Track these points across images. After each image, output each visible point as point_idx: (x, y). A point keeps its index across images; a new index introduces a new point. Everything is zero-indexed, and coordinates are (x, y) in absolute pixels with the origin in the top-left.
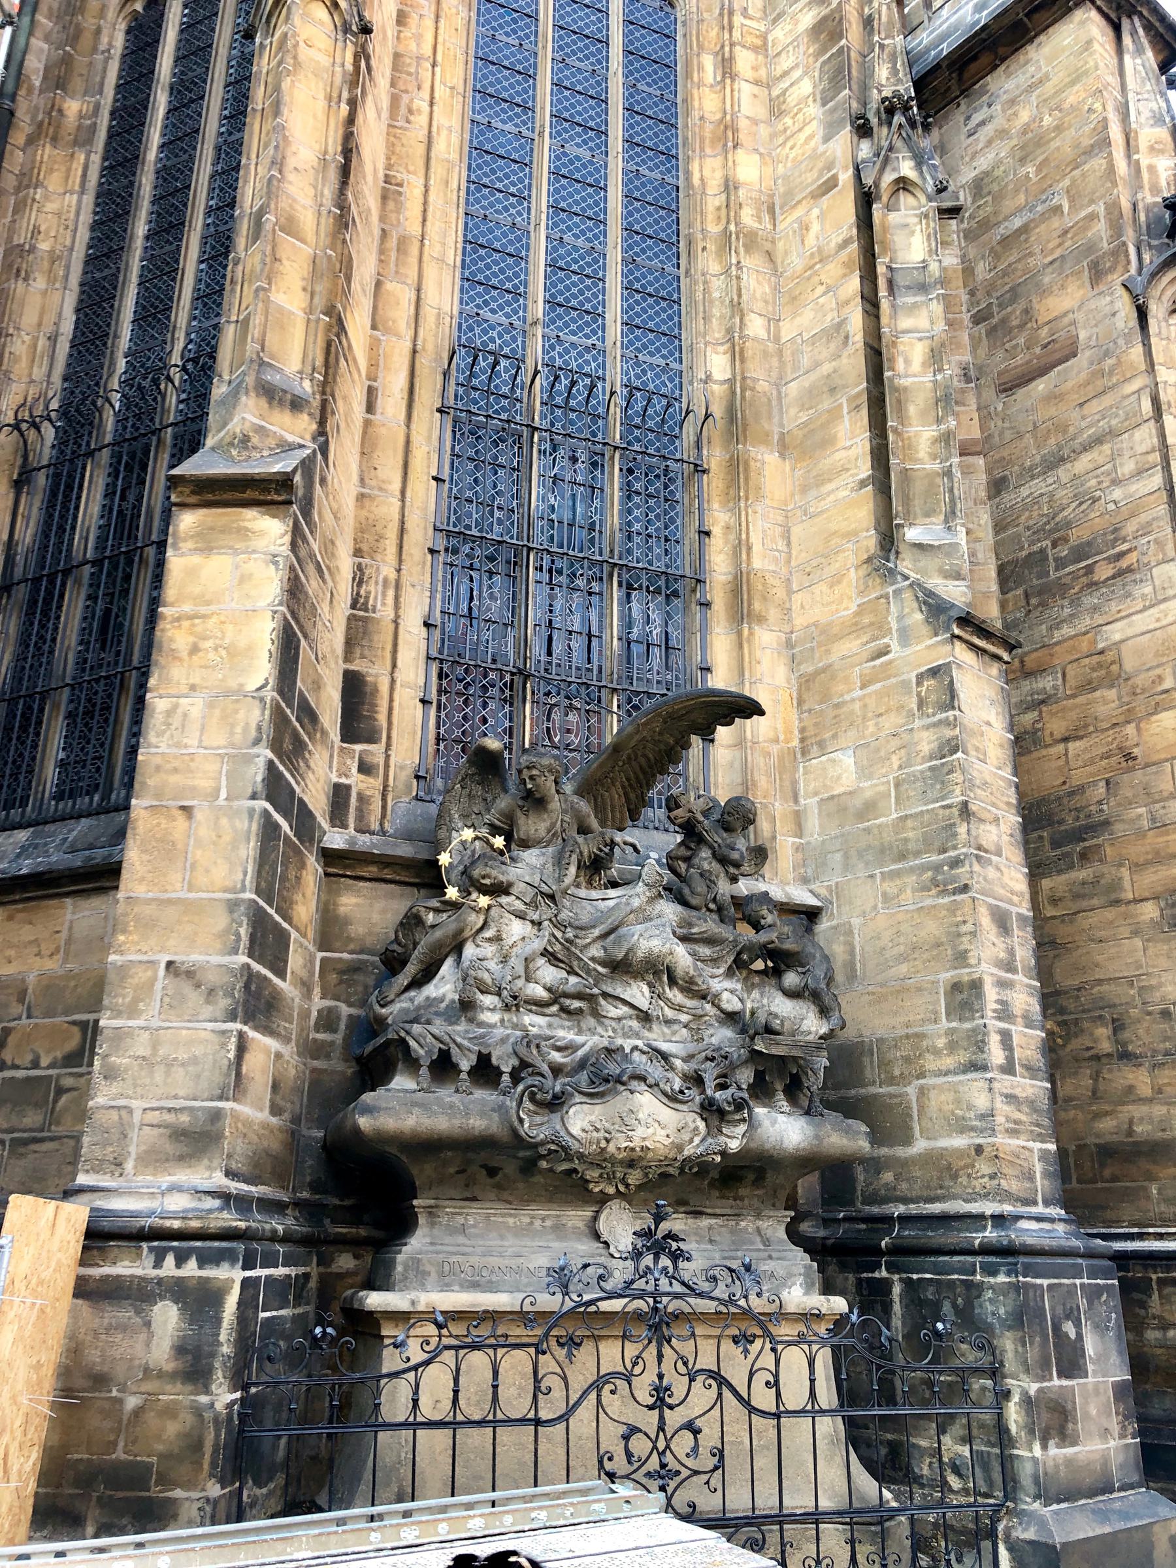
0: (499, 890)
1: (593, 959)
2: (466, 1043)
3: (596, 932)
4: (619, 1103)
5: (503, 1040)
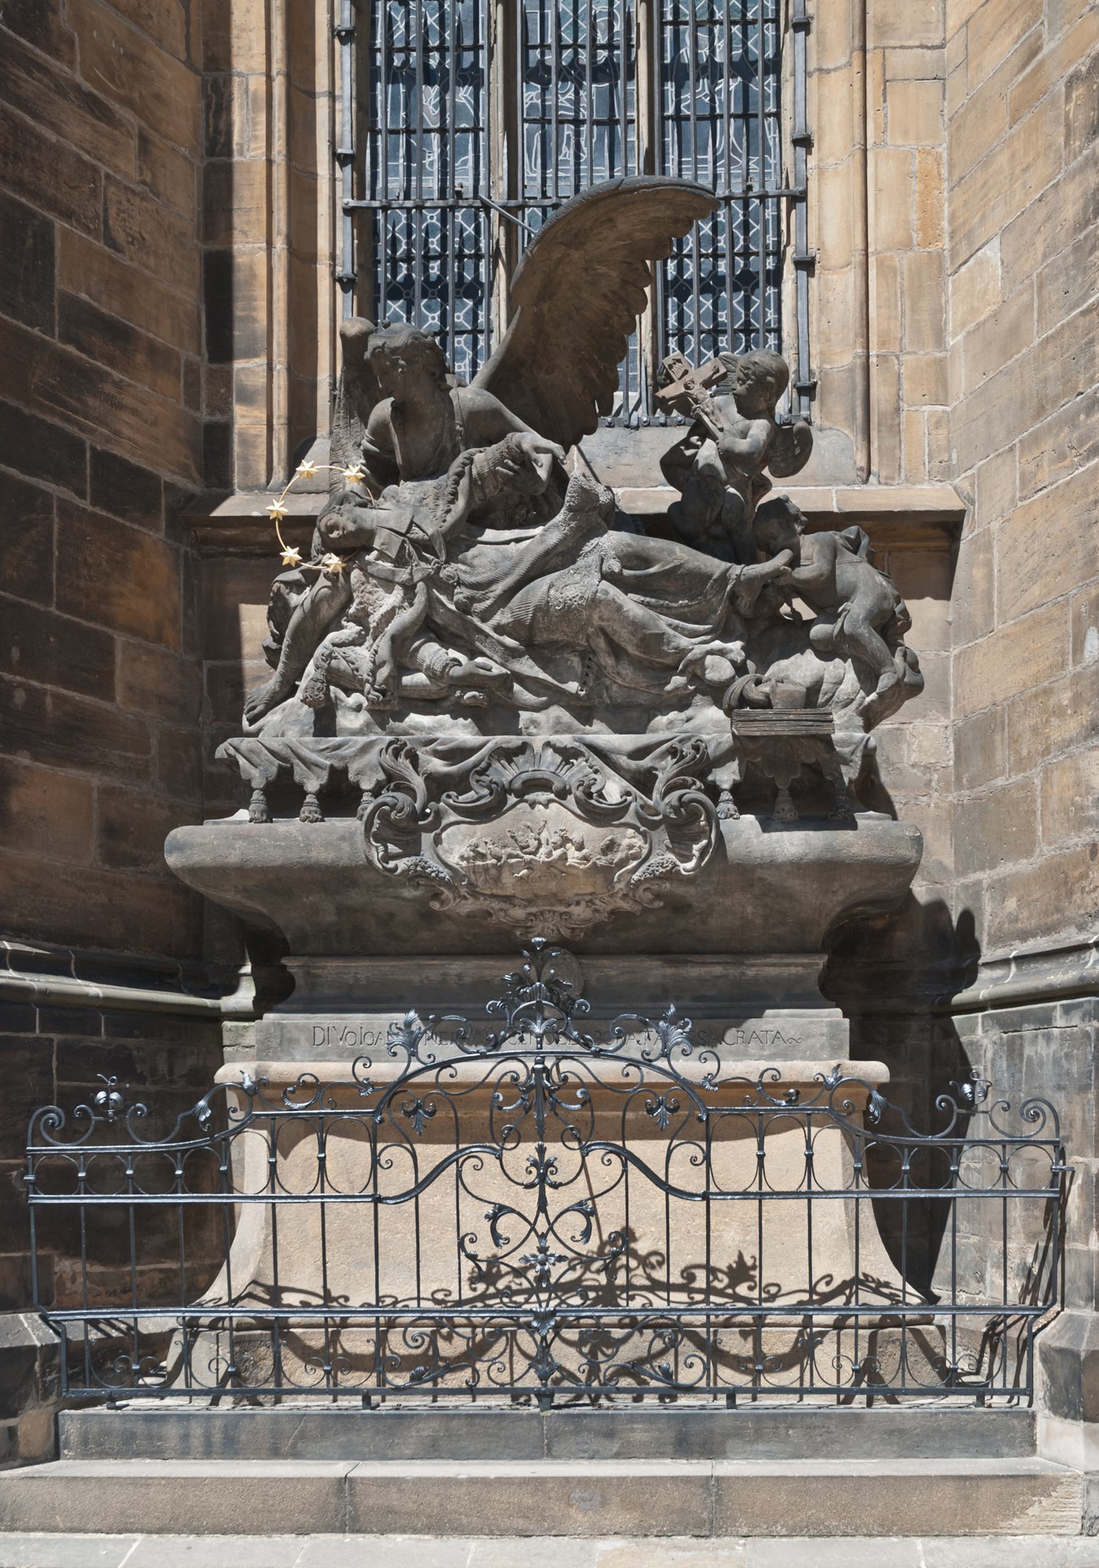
0: (355, 546)
1: (499, 629)
2: (315, 757)
3: (499, 588)
4: (517, 817)
5: (366, 748)
